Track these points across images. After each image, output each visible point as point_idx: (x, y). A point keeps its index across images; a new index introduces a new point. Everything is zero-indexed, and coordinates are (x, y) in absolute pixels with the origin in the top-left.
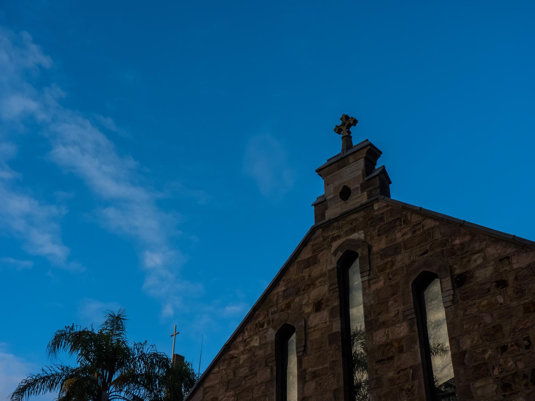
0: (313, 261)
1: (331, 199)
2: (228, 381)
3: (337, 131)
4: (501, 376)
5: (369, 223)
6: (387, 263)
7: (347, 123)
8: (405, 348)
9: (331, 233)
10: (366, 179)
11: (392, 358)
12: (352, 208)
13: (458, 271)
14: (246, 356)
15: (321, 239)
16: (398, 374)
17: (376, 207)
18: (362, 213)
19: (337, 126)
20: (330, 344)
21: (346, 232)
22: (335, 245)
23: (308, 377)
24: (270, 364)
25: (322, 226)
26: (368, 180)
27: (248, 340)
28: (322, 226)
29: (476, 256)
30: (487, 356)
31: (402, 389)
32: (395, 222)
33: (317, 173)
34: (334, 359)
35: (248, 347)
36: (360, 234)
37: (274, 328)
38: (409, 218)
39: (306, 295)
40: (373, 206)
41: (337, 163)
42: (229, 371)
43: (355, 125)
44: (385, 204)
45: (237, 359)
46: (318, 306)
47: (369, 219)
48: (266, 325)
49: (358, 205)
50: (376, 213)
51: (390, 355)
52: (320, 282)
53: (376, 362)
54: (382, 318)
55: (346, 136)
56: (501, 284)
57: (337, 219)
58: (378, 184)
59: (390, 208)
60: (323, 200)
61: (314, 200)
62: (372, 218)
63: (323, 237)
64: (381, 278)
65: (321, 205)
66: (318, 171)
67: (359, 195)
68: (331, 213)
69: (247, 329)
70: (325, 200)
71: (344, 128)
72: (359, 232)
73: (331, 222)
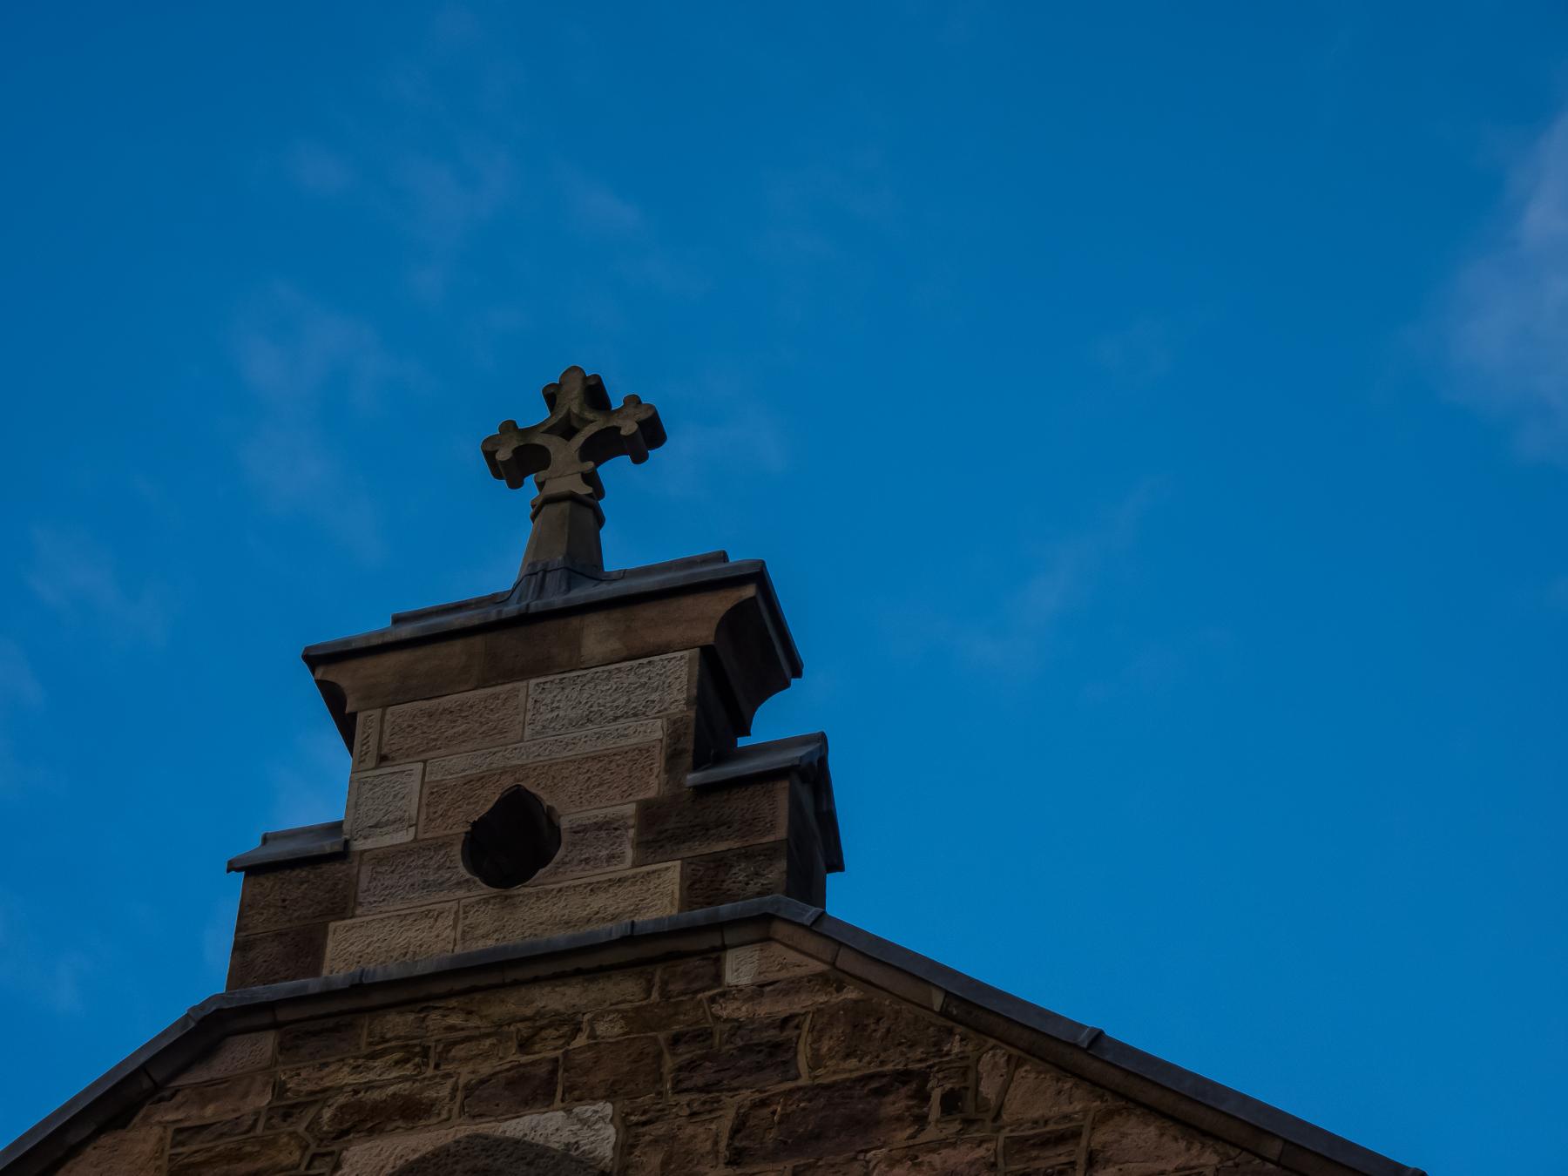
1: (385, 857)
3: (503, 455)
5: (669, 1063)
7: (584, 434)
9: (345, 1077)
10: (693, 778)
12: (560, 936)
15: (265, 1100)
17: (740, 968)
18: (625, 990)
19: (509, 427)
21: (469, 1089)
25: (283, 1015)
26: (702, 790)
28: (283, 1015)
32: (880, 1092)
33: (307, 681)
36: (584, 1122)
38: (989, 1089)
40: (718, 962)
41: (478, 642)
43: (639, 458)
44: (819, 967)
47: (676, 1040)
49: (616, 930)
50: (727, 1010)
55: (572, 497)
57: (416, 990)
58: (782, 833)
59: (851, 994)
60: (329, 845)
61: (249, 845)
62: (703, 1035)
63: (280, 1090)
65: (296, 883)
66: (314, 659)
67: (624, 868)
68: (356, 947)
70: (343, 855)
71: (564, 453)
72: (585, 1110)
73: (366, 996)
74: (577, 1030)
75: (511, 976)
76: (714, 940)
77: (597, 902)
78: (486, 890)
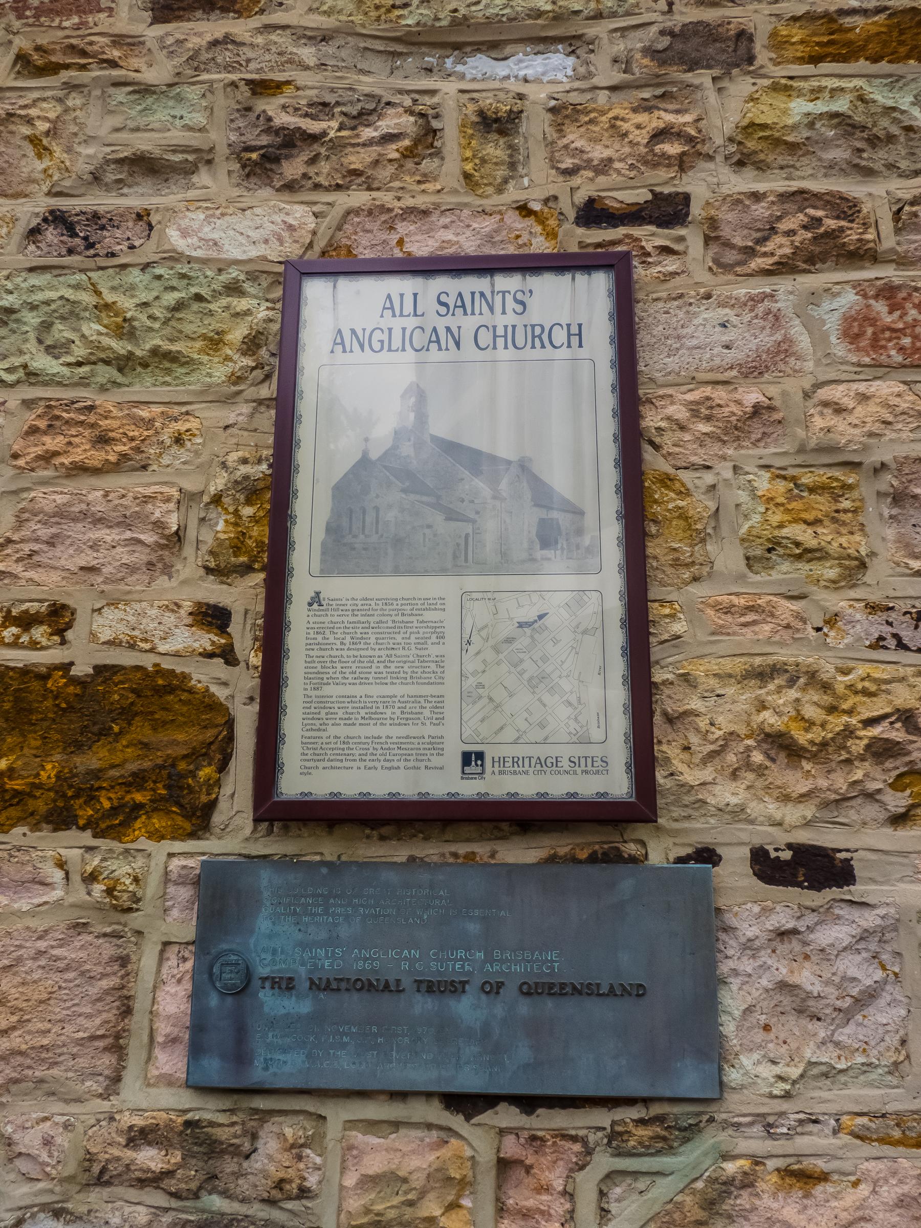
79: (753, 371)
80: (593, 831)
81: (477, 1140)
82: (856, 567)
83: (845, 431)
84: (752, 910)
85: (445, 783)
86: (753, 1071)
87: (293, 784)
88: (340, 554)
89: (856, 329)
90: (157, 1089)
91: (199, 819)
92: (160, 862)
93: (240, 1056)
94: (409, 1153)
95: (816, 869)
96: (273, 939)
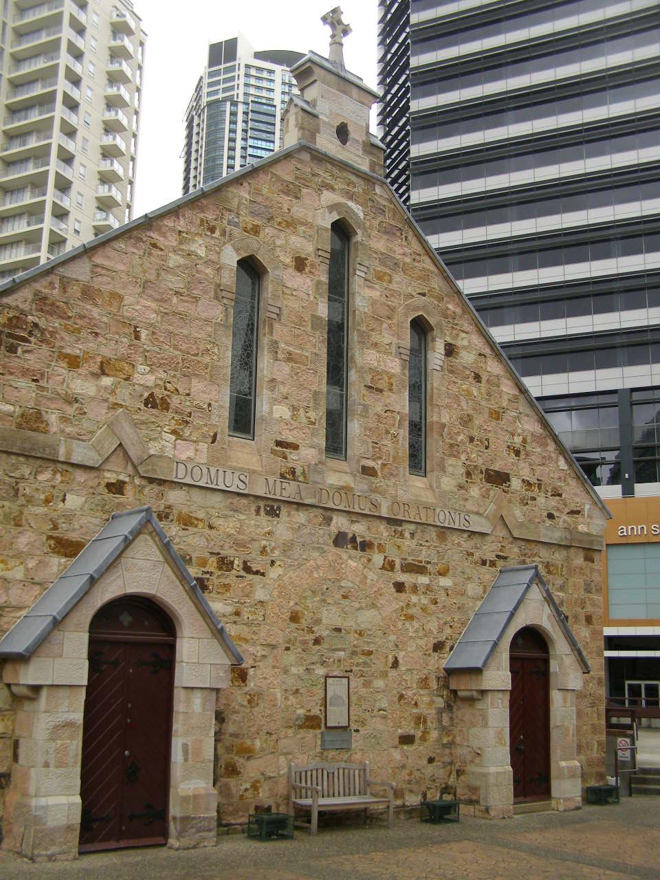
0: (292, 191)
2: (146, 282)
4: (467, 463)
6: (385, 273)
8: (394, 387)
11: (381, 391)
13: (449, 339)
14: (181, 261)
16: (385, 412)
20: (312, 327)
22: (328, 197)
23: (280, 356)
24: (225, 301)
25: (313, 152)
27: (185, 235)
29: (463, 335)
30: (460, 438)
31: (387, 432)
34: (315, 351)
35: (183, 247)
37: (237, 250)
39: (283, 234)
42: (149, 265)
45: (163, 253)
46: (300, 264)
48: (217, 234)
51: (380, 386)
52: (304, 232)
53: (365, 386)
54: (375, 337)
56: (477, 378)
64: (377, 286)
69: (184, 216)
74: (355, 187)
75: (348, 168)
76: (375, 181)
77: (357, 159)
78: (339, 143)
79: (356, 688)
80: (345, 728)
81: (338, 752)
82: (361, 706)
83: (361, 693)
84: (354, 734)
85: (337, 725)
86: (353, 746)
87: (328, 725)
88: (330, 705)
89: (363, 684)
90: (318, 749)
91: (320, 728)
92: (318, 731)
93: (324, 745)
94: (333, 753)
95: (357, 731)
96: (327, 738)
